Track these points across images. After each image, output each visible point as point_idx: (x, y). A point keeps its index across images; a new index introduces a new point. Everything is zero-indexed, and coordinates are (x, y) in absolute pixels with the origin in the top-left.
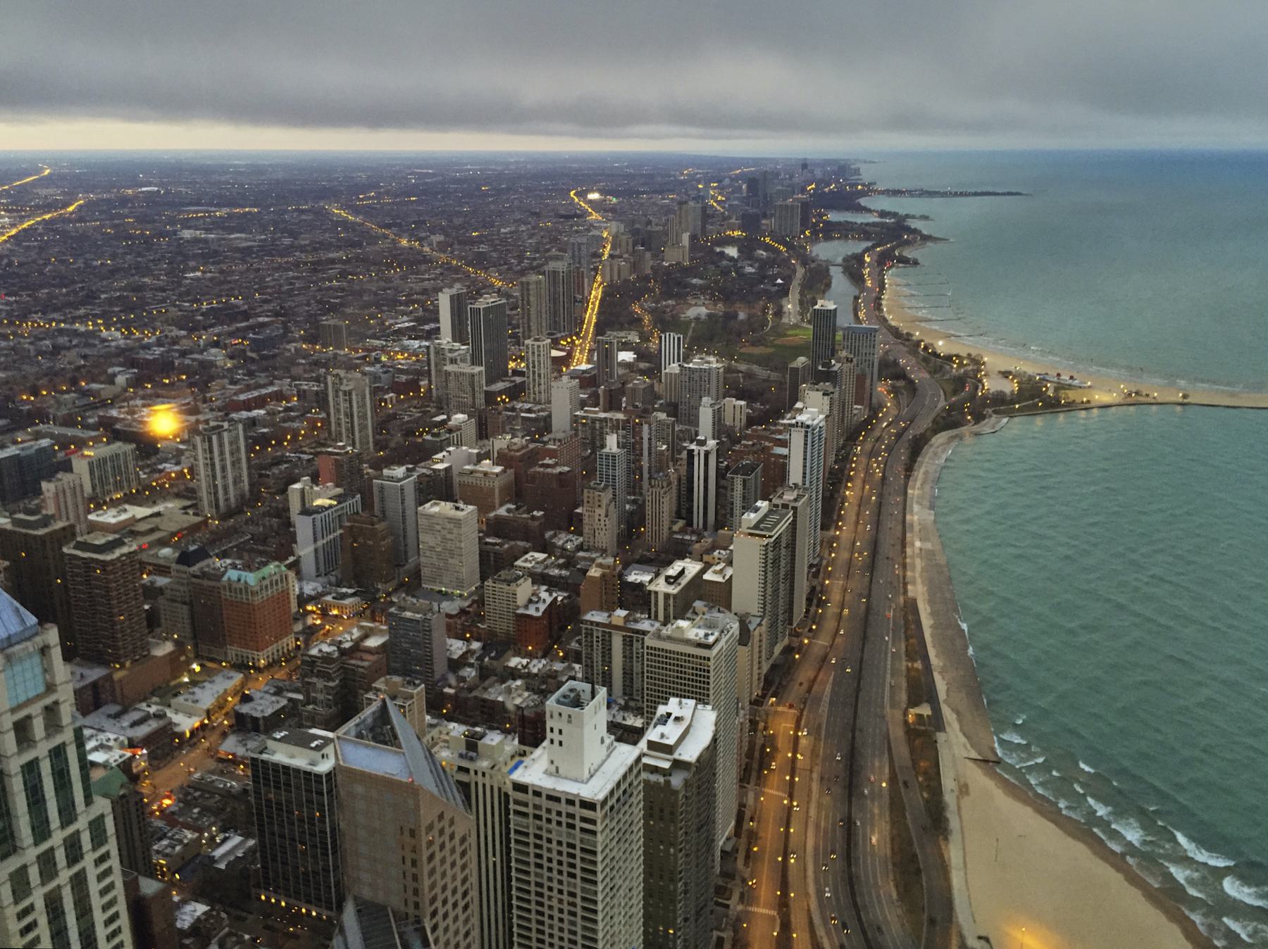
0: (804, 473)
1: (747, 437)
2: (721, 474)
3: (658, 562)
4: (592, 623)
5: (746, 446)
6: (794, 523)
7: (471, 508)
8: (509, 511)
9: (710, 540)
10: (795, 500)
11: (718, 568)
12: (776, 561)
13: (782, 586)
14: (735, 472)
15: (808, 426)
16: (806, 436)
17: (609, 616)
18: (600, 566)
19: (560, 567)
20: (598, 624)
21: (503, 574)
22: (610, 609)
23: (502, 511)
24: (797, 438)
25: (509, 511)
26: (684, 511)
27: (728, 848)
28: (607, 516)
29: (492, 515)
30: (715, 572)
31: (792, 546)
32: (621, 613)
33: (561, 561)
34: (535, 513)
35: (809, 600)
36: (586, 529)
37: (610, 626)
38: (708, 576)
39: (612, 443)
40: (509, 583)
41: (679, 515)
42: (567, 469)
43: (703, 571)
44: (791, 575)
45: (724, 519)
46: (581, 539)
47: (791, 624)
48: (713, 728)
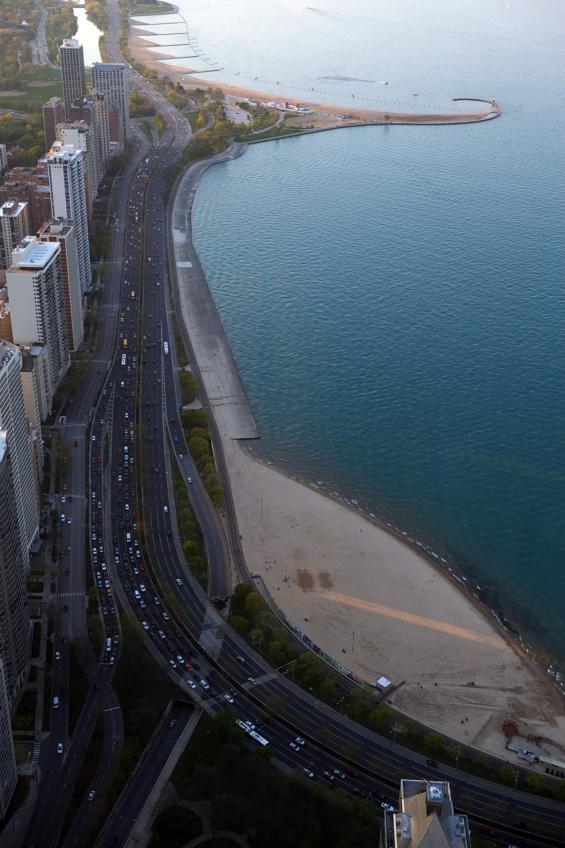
0: (68, 208)
5: (9, 187)
10: (62, 233)
12: (49, 291)
13: (59, 314)
15: (66, 162)
16: (65, 172)
27: (36, 550)
31: (63, 276)
35: (87, 324)
44: (66, 305)
47: (73, 349)
48: (5, 445)
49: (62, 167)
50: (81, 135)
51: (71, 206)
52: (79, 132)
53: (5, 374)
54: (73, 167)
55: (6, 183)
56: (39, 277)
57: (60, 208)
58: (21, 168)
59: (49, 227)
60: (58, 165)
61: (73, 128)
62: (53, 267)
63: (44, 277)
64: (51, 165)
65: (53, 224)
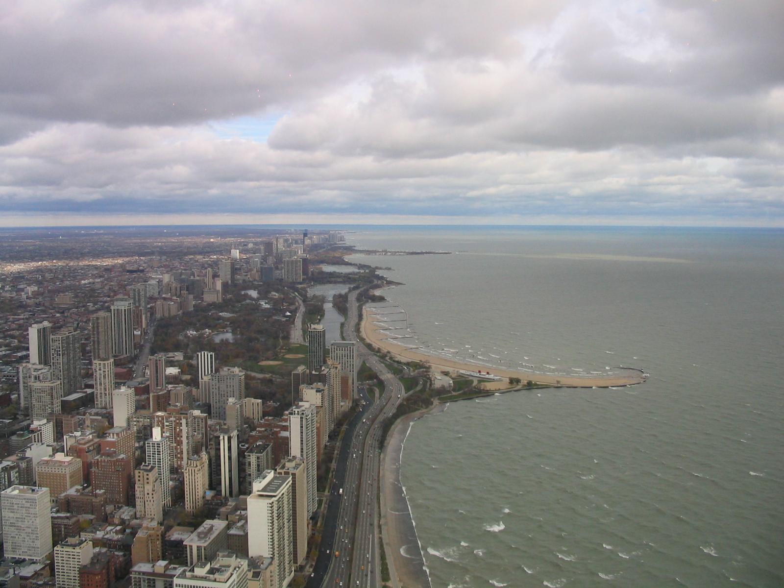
0: (302, 449)
1: (261, 426)
2: (241, 454)
3: (193, 523)
4: (139, 573)
5: (260, 432)
6: (294, 485)
7: (44, 489)
8: (77, 491)
9: (234, 504)
11: (239, 524)
14: (251, 451)
16: (301, 421)
17: (153, 566)
18: (147, 528)
19: (117, 532)
20: (144, 573)
21: (70, 540)
22: (154, 561)
23: (72, 492)
24: (295, 422)
25: (77, 491)
26: (214, 483)
28: (153, 491)
29: (63, 495)
30: (238, 528)
32: (162, 563)
33: (119, 528)
34: (98, 491)
36: (138, 502)
37: (153, 574)
38: (233, 531)
39: (157, 433)
40: (74, 546)
41: (211, 487)
42: (122, 456)
43: (228, 527)
45: (243, 488)
46: (134, 510)
47: (295, 561)
49: (299, 418)
50: (318, 394)
51: (305, 448)
52: (317, 391)
53: (234, 580)
54: (308, 418)
55: (258, 429)
56: (273, 503)
57: (295, 449)
58: (270, 418)
59: (285, 464)
60: (296, 415)
61: (312, 388)
62: (284, 495)
63: (277, 503)
64: (291, 416)
65: (288, 461)
